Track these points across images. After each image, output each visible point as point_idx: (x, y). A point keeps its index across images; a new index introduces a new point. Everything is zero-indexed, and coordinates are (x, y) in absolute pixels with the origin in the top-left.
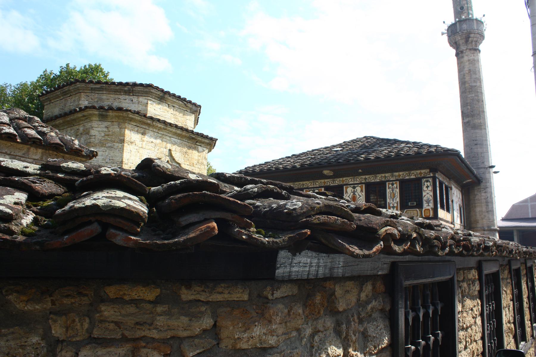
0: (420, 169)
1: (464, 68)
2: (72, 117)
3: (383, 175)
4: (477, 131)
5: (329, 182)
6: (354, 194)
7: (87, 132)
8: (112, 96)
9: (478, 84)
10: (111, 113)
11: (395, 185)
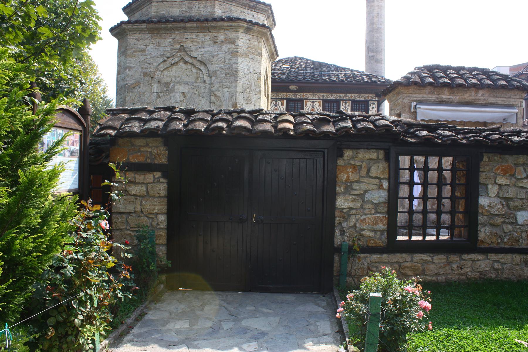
0: (369, 93)
1: (373, 11)
2: (213, 24)
3: (338, 95)
4: (379, 64)
5: (291, 96)
6: (313, 107)
7: (232, 42)
8: (239, 8)
9: (383, 27)
10: (256, 28)
11: (348, 104)
